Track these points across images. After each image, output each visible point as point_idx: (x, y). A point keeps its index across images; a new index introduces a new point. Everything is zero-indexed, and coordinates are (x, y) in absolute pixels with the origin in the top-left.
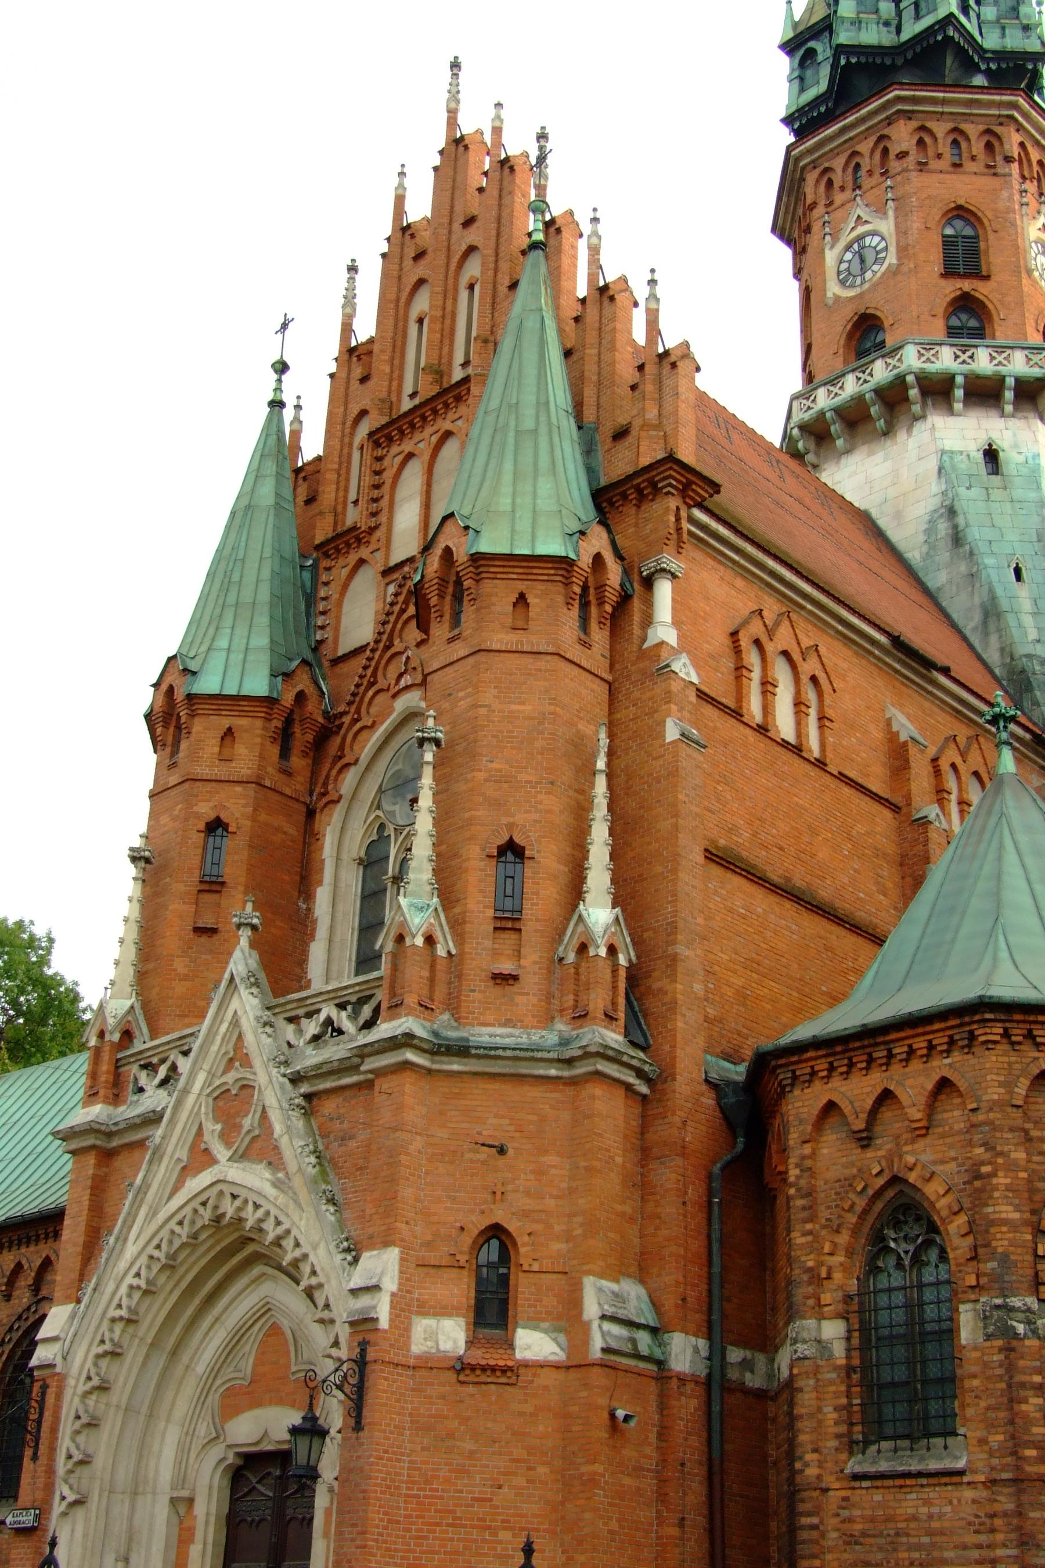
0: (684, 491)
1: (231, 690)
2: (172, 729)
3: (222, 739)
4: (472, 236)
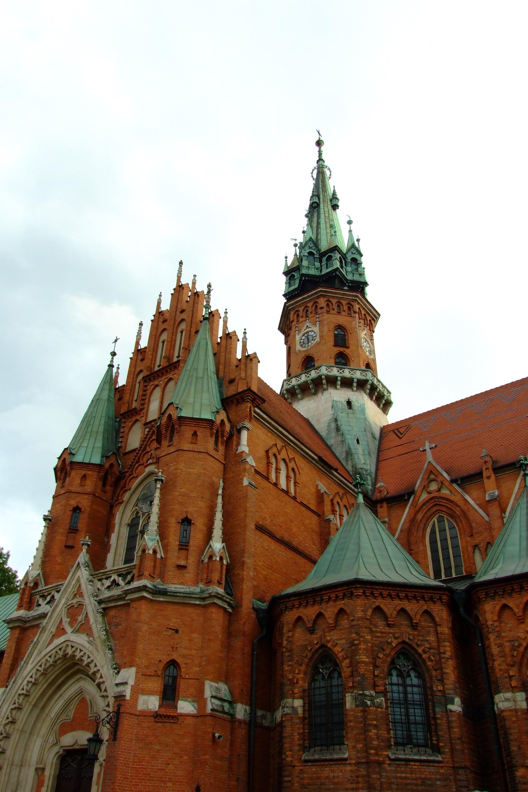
0: (253, 401)
1: (87, 461)
2: (63, 474)
3: (82, 478)
4: (183, 316)
